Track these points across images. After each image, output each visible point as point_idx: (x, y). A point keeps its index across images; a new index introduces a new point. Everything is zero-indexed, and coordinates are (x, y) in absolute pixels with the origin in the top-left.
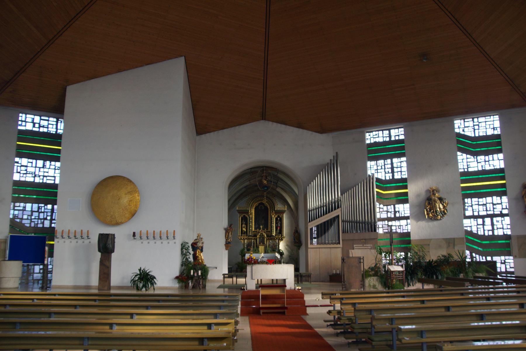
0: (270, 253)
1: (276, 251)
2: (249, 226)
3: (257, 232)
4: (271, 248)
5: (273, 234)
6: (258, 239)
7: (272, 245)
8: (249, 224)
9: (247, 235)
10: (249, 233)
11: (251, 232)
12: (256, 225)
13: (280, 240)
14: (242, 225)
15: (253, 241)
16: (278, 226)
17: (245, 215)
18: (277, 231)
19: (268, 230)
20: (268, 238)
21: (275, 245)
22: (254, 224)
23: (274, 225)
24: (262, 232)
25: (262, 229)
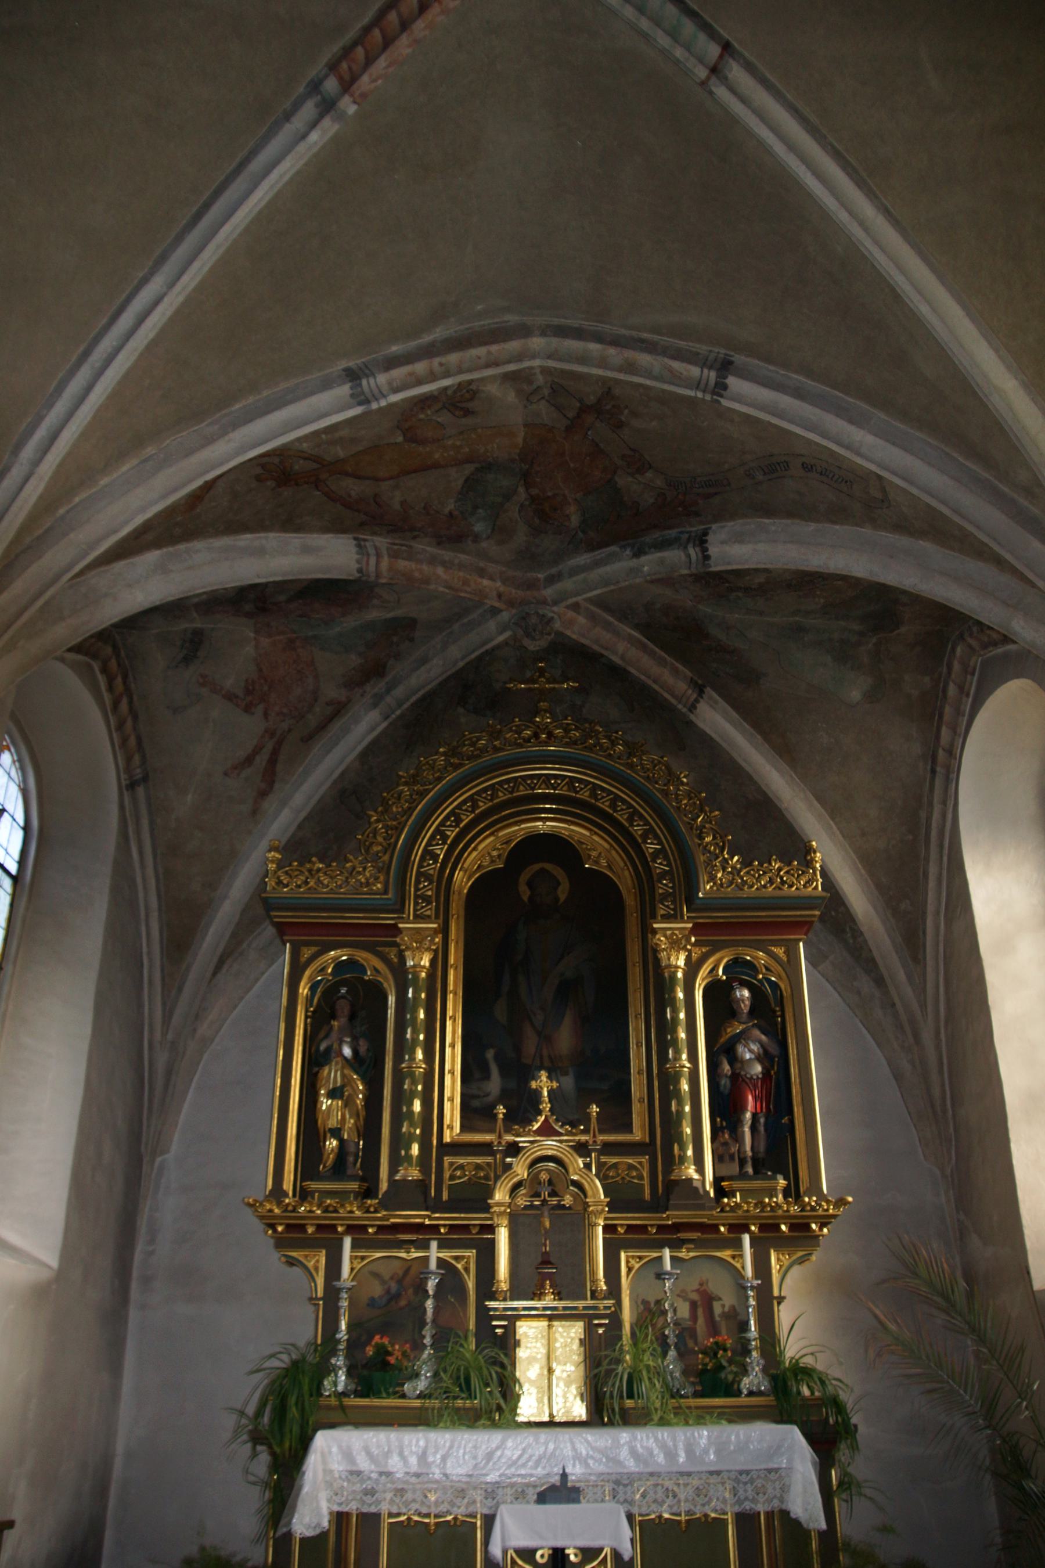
0: (663, 1422)
1: (746, 1383)
2: (399, 1077)
3: (485, 1149)
4: (672, 1353)
5: (692, 1172)
6: (503, 1237)
7: (684, 1311)
8: (403, 1048)
9: (369, 1192)
10: (395, 1163)
11: (415, 1149)
12: (486, 1075)
13: (783, 1243)
14: (314, 1062)
15: (441, 1262)
16: (736, 1078)
17: (369, 960)
18: (738, 1138)
19: (628, 1128)
20: (635, 1219)
21: (717, 1309)
22: (454, 1057)
23: (693, 1057)
24: (550, 1145)
25: (546, 1106)
